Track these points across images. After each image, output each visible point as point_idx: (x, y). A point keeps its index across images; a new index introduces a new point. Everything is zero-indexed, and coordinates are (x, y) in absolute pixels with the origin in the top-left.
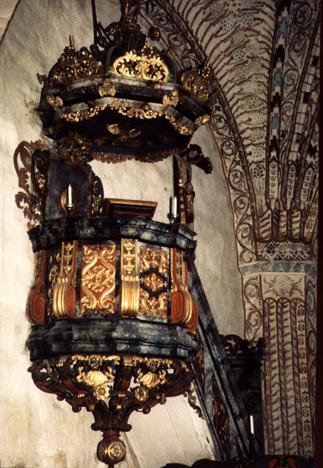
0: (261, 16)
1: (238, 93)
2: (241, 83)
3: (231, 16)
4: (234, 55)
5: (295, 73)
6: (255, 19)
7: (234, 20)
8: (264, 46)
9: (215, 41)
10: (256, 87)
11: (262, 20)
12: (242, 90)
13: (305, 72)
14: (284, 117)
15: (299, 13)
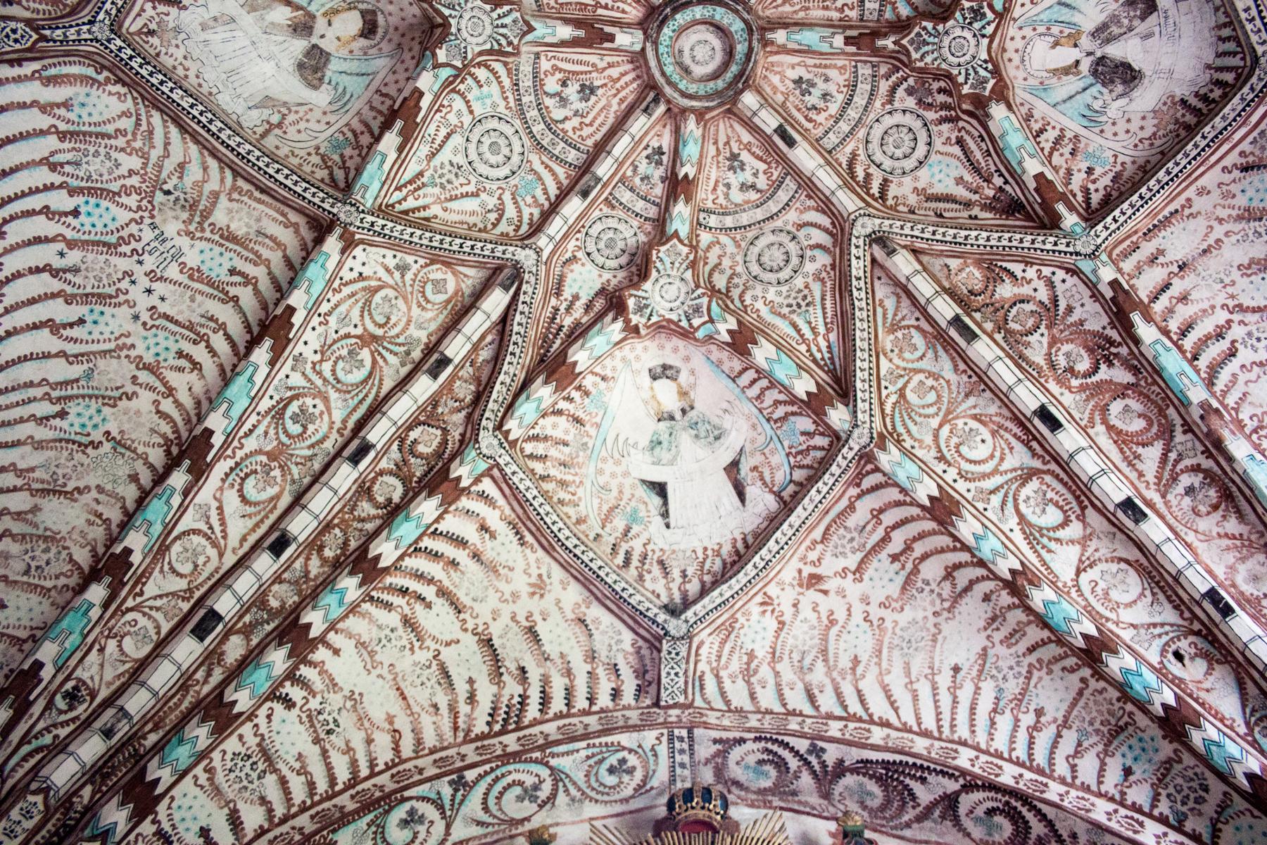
0: (199, 353)
1: (19, 516)
2: (45, 492)
3: (125, 311)
4: (73, 408)
5: (212, 553)
6: (180, 354)
7: (129, 326)
8: (166, 428)
9: (44, 341)
10: (80, 522)
11: (196, 366)
12: (36, 509)
13: (242, 563)
14: (112, 645)
15: (294, 407)
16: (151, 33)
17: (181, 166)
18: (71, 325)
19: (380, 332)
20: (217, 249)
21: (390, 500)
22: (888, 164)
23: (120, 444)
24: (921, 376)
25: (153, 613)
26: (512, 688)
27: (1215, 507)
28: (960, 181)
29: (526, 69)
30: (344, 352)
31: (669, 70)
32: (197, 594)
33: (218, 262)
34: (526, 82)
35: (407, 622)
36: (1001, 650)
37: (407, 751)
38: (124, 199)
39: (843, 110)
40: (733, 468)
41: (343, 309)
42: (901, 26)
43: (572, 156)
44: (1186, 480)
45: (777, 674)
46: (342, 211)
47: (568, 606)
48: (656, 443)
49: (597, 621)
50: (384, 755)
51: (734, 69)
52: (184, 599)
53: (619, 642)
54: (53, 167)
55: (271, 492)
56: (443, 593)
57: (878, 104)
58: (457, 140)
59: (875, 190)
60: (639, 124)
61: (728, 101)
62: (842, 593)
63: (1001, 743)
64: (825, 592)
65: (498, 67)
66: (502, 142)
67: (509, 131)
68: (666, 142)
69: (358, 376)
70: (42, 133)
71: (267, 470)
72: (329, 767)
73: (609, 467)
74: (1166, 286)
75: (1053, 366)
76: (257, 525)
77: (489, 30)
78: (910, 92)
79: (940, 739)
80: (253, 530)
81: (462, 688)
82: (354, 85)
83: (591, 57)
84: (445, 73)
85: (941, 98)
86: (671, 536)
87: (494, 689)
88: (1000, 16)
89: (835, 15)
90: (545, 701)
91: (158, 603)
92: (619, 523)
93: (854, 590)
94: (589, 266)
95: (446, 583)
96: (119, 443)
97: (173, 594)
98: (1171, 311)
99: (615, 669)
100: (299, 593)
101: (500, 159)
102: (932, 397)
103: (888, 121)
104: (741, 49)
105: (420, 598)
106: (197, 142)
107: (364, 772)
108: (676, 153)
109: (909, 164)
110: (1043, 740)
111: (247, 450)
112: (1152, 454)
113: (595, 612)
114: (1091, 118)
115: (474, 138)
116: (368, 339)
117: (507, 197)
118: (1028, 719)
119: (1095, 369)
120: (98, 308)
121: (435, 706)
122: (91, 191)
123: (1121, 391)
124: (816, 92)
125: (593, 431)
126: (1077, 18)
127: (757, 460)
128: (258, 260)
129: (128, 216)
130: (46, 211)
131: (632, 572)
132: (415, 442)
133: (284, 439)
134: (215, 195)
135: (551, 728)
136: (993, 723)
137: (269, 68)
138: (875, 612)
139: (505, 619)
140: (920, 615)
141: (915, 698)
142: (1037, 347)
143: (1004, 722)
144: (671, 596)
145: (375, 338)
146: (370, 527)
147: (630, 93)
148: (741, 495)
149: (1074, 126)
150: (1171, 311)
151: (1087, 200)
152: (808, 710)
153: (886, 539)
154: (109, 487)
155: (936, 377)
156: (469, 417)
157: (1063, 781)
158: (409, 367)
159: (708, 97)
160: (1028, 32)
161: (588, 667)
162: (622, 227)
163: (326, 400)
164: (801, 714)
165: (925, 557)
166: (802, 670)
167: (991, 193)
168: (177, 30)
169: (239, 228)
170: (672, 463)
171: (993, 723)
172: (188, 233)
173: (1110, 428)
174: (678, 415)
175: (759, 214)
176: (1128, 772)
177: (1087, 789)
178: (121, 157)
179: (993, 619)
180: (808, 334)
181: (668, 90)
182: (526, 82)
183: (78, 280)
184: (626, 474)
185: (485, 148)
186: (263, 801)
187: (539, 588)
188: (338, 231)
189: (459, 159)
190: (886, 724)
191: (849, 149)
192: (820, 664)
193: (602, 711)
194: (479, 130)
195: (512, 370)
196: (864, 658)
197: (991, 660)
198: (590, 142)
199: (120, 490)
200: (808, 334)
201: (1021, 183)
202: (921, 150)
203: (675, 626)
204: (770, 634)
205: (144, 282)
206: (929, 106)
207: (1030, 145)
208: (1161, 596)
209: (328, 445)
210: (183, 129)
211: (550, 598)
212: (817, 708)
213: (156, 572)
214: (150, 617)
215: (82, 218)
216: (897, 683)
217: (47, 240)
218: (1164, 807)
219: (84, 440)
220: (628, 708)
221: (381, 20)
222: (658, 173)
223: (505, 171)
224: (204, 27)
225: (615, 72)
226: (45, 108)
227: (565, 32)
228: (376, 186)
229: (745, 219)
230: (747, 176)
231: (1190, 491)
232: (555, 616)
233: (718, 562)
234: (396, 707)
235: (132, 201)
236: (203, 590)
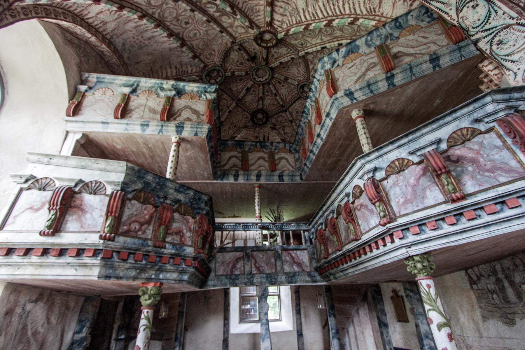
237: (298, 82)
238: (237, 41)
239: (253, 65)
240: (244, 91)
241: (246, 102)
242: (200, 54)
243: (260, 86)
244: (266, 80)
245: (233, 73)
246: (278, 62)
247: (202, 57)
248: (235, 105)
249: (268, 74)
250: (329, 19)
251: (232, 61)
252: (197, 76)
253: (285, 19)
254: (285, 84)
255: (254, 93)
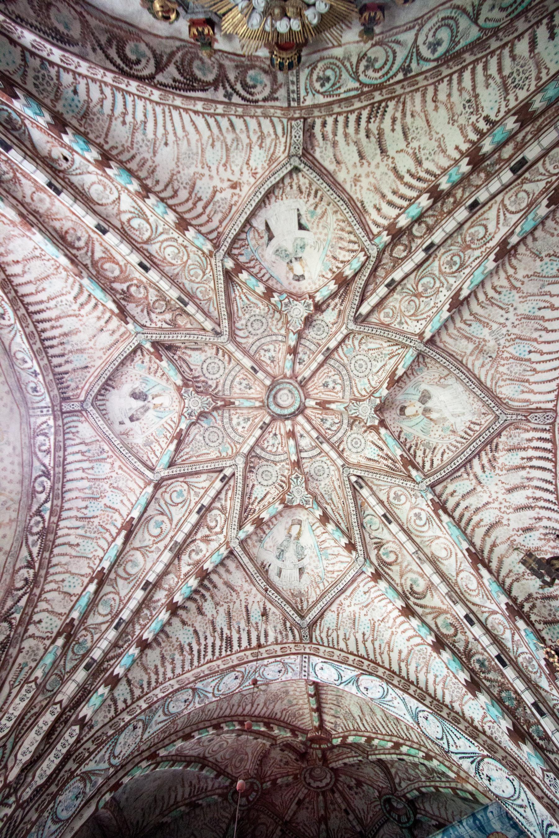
5: (507, 202)
6: (500, 293)
7: (520, 306)
8: (514, 261)
11: (494, 288)
13: (493, 196)
15: (455, 268)
16: (484, 414)
17: (483, 366)
18: (544, 308)
19: (413, 298)
20: (475, 334)
21: (419, 224)
22: (217, 361)
23: (537, 256)
24: (197, 280)
25: (544, 172)
26: (373, 127)
27: (66, 232)
28: (190, 356)
29: (347, 393)
30: (429, 291)
31: (296, 392)
32: (519, 181)
33: (476, 330)
34: (348, 389)
35: (419, 163)
36: (147, 156)
37: (431, 89)
38: (509, 356)
39: (234, 379)
40: (271, 238)
41: (427, 309)
42: (216, 409)
43: (332, 362)
44: (81, 244)
45: (248, 137)
46: (422, 348)
47: (344, 170)
48: (303, 247)
49: (331, 163)
50: (443, 87)
51: (273, 392)
52: (527, 179)
53: (321, 152)
54: (535, 370)
55: (472, 230)
56: (401, 178)
57: (222, 382)
58: (375, 370)
59: (221, 351)
60: (307, 374)
61: (275, 382)
62: (222, 180)
63: (140, 104)
64: (229, 180)
65: (357, 395)
66: (358, 368)
67: (355, 372)
68: (297, 366)
69: (425, 280)
70: (535, 383)
71: (472, 241)
72: (473, 80)
73: (322, 237)
74: (107, 322)
75: (145, 288)
76: (482, 214)
77: (360, 409)
78: (210, 386)
79: (169, 105)
80: (484, 212)
81: (398, 127)
82: (411, 390)
83: (324, 397)
84: (377, 395)
85: (199, 385)
86: (296, 205)
87: (382, 126)
88: (182, 414)
89: (238, 411)
90: (358, 120)
91: (540, 177)
92: (319, 211)
93: (216, 182)
94: (327, 321)
95: (398, 183)
96: (537, 256)
97: (531, 181)
98: (103, 313)
99: (324, 137)
100: (469, 180)
101: (359, 362)
102: (192, 272)
103: (217, 376)
104: (271, 399)
105: (412, 175)
106: (475, 375)
107: (455, 77)
108: (294, 363)
109: (208, 361)
110: (119, 108)
111: (480, 250)
112: (98, 254)
113: (331, 167)
114: (145, 381)
115: (368, 370)
116: (418, 295)
117: (357, 348)
118: (129, 118)
119: (128, 288)
120: (530, 314)
121: (412, 116)
122: (521, 360)
123: (116, 279)
124: (244, 385)
125: (329, 253)
126: (155, 413)
127: (261, 242)
128: (459, 330)
129: (509, 349)
130: (542, 353)
131: (314, 188)
132: (404, 251)
133: (462, 254)
134: (471, 354)
135: (357, 105)
136: (145, 116)
137: (442, 398)
138: (206, 171)
139: (373, 163)
140: (186, 171)
141: (183, 127)
142: (153, 296)
143: (140, 117)
144: (297, 176)
145: (415, 296)
146: (430, 213)
147: (310, 384)
148: (267, 225)
149: (151, 377)
150: (103, 313)
151: (142, 352)
152: (233, 118)
153: (205, 208)
154: (548, 236)
155: (191, 281)
156: (380, 261)
157: (106, 84)
158: (403, 283)
159: (282, 383)
160: (172, 408)
161: (336, 138)
162: (315, 336)
163: (440, 270)
164: (237, 116)
165: (187, 200)
166: (237, 139)
167: (178, 353)
168: (474, 414)
169: (464, 342)
170: (296, 239)
171: (145, 116)
172: (484, 340)
173: (117, 264)
174: (293, 260)
175: (263, 341)
176: (75, 92)
177: (94, 80)
178: (506, 371)
179: (153, 172)
180: (242, 296)
181: (297, 385)
182: (348, 389)
183: (536, 326)
184: (315, 234)
185: (364, 366)
186: (513, 58)
187: (356, 179)
188: (425, 340)
189: (374, 363)
190: (196, 112)
191: (231, 365)
192: (229, 143)
193: (331, 115)
194: (366, 373)
195: (360, 282)
196: (209, 147)
197: (151, 150)
198: (325, 367)
199: (543, 234)
200: (242, 296)
201: (168, 357)
202: (205, 366)
203: (296, 162)
204: (252, 158)
205: (508, 323)
206: (203, 382)
207: (166, 371)
208: (80, 189)
209: (442, 250)
210: (479, 380)
211: (352, 174)
212: (229, 120)
213: (537, 193)
214: (546, 170)
215: (528, 350)
216: (193, 136)
217: (545, 342)
218: (53, 71)
219: (553, 258)
220: (319, 117)
221: (398, 412)
222: (300, 356)
223: (357, 358)
224: (464, 414)
225: (316, 391)
226: (532, 391)
227: (332, 406)
228: (408, 356)
229: (268, 339)
230: (268, 354)
231: (79, 239)
232: (350, 165)
233: (276, 194)
234: (433, 115)
235: (505, 355)
236: (516, 183)
237: (379, 792)
238: (278, 742)
239: (304, 766)
240: (294, 806)
241: (298, 824)
242: (227, 766)
243: (318, 795)
244: (327, 784)
245: (274, 782)
246: (340, 762)
247: (229, 770)
248: (280, 834)
249: (328, 776)
250: (395, 739)
251: (272, 761)
252: (220, 795)
253: (339, 721)
254: (359, 790)
255: (311, 807)
